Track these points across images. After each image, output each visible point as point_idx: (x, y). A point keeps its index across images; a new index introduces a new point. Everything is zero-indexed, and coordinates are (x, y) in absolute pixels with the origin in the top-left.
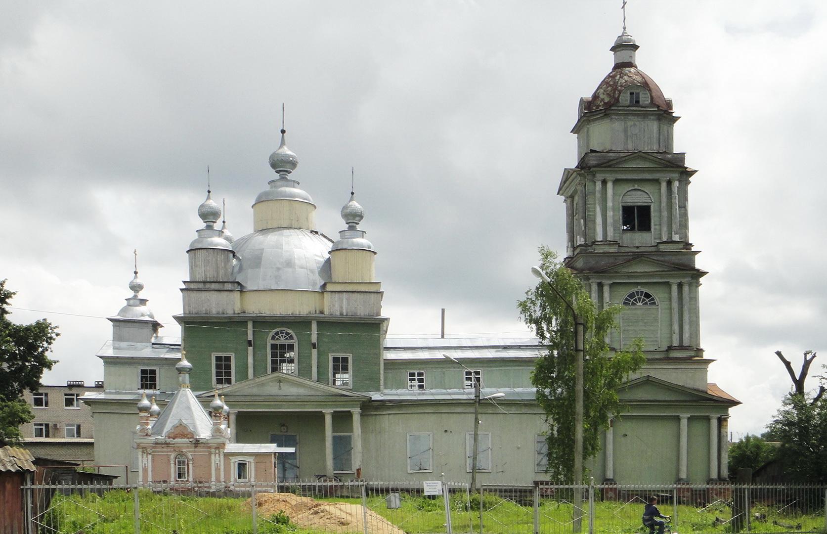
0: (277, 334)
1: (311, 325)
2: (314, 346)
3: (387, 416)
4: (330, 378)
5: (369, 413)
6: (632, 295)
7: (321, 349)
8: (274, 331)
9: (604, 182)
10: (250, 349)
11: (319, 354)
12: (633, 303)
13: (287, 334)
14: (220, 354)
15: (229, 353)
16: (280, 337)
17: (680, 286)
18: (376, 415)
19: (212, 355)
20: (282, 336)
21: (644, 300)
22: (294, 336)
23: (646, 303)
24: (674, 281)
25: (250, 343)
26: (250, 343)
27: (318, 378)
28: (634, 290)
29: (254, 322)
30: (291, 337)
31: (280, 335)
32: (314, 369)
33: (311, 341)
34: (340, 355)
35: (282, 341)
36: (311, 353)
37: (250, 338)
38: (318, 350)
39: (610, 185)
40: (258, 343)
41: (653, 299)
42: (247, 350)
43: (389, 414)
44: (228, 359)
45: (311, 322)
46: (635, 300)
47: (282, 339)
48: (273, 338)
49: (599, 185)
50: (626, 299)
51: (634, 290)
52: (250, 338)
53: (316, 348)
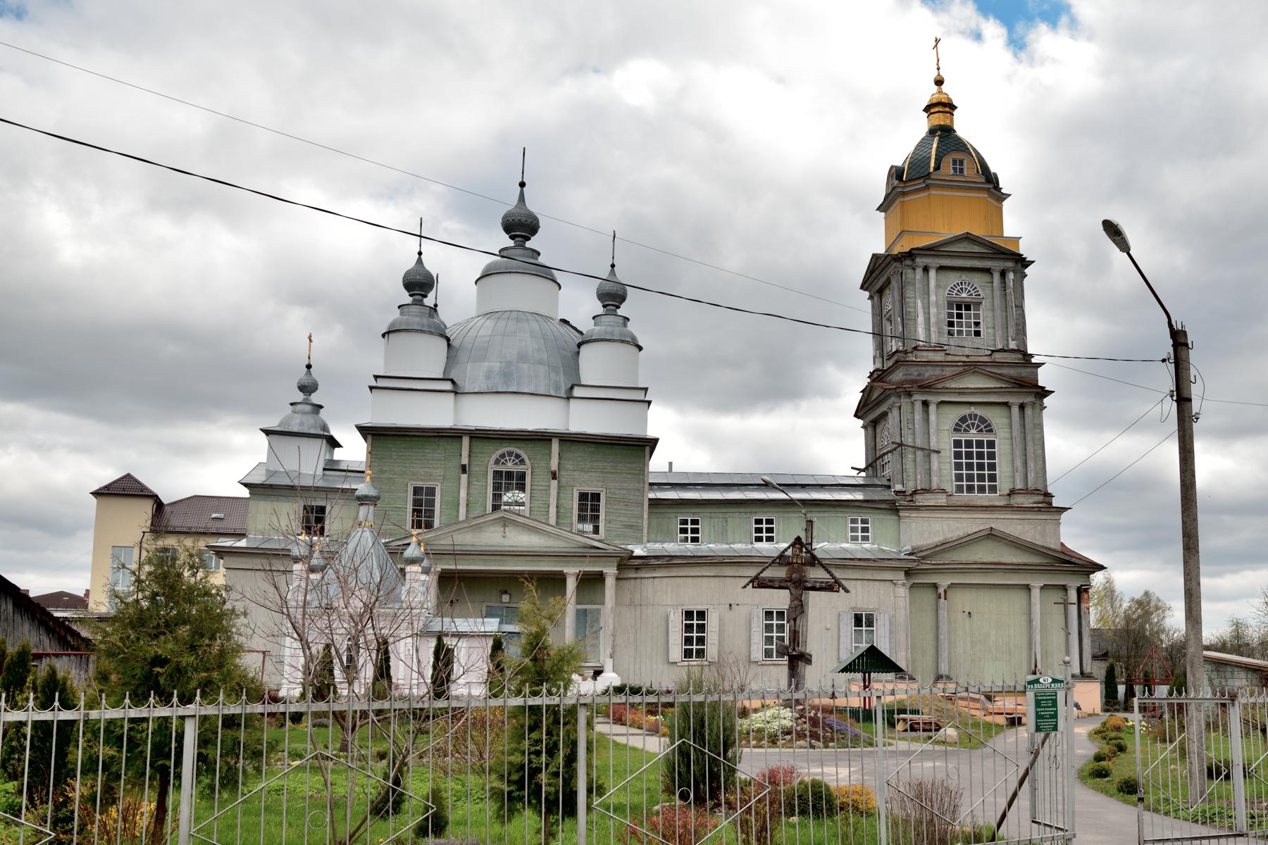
0: (503, 456)
2: (554, 476)
7: (563, 480)
10: (464, 477)
11: (559, 487)
13: (518, 456)
14: (420, 484)
15: (431, 483)
16: (506, 461)
18: (636, 578)
19: (409, 485)
20: (510, 460)
22: (527, 461)
25: (464, 469)
26: (464, 469)
27: (557, 523)
29: (471, 437)
30: (522, 462)
31: (507, 458)
32: (553, 510)
33: (549, 467)
34: (590, 489)
35: (510, 466)
36: (549, 486)
37: (465, 461)
38: (559, 482)
40: (474, 469)
42: (460, 478)
43: (654, 578)
44: (431, 491)
45: (551, 440)
47: (510, 464)
48: (497, 462)
52: (465, 461)
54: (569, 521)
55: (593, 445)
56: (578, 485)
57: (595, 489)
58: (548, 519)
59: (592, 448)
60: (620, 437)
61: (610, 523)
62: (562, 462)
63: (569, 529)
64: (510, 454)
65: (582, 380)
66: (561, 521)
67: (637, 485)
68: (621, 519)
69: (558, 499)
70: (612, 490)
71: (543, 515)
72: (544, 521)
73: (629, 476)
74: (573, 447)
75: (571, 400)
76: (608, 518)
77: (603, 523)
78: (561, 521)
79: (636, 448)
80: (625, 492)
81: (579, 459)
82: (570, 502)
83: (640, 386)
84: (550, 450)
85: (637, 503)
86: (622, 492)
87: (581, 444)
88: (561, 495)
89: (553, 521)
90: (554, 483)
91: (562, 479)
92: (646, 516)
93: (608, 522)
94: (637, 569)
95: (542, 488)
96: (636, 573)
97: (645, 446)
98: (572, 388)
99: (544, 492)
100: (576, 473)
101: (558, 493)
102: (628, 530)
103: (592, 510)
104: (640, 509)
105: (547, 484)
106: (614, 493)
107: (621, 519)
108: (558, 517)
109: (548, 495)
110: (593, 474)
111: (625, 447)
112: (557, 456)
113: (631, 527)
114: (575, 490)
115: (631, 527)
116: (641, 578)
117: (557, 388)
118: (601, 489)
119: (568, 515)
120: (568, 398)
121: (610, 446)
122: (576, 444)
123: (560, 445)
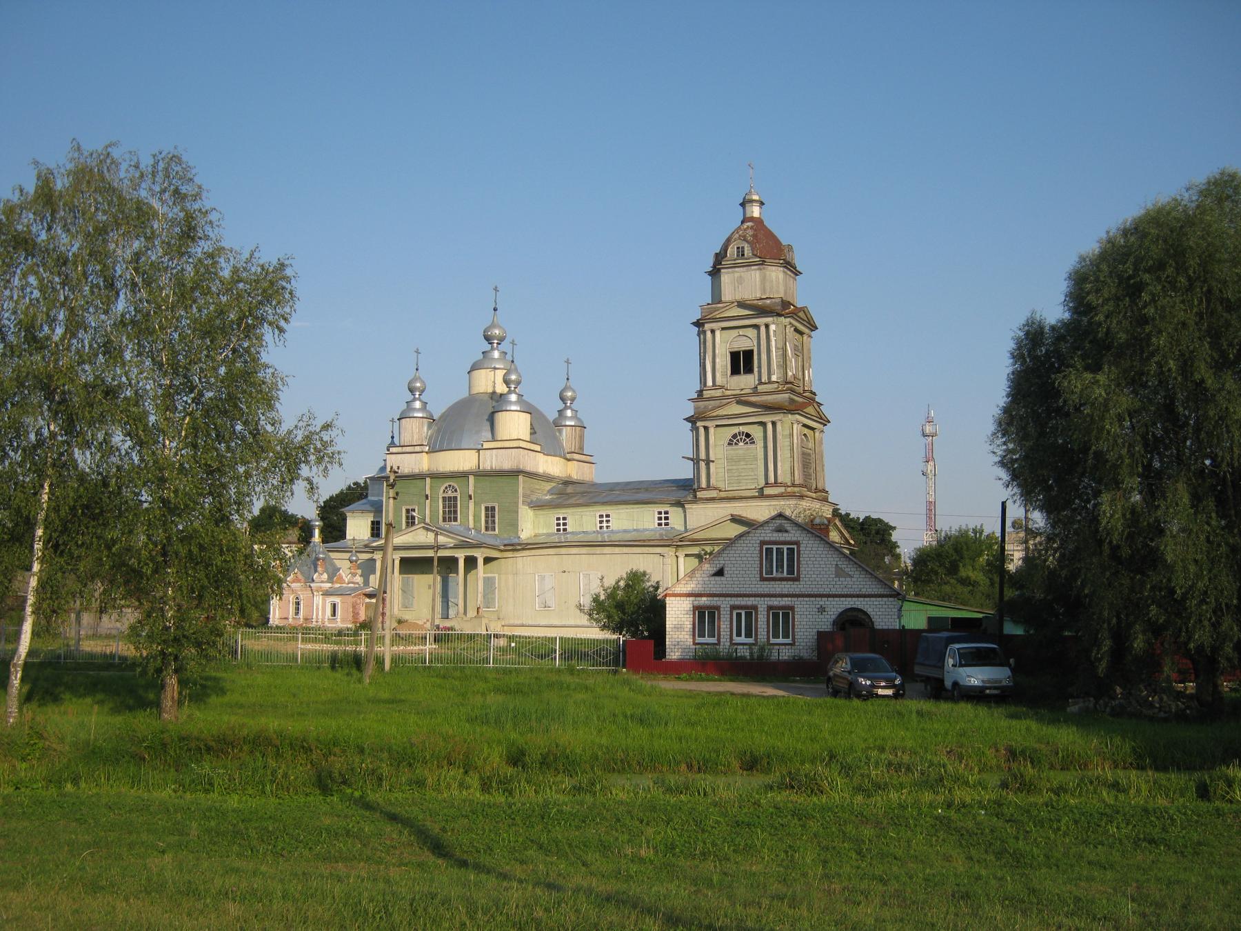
0: (446, 488)
6: (735, 436)
8: (447, 484)
9: (713, 331)
12: (736, 444)
17: (774, 424)
21: (745, 440)
23: (747, 443)
24: (767, 419)
28: (736, 430)
30: (456, 491)
35: (450, 494)
39: (718, 333)
41: (752, 439)
46: (738, 441)
47: (450, 492)
49: (709, 334)
50: (730, 440)
51: (736, 430)
64: (450, 486)
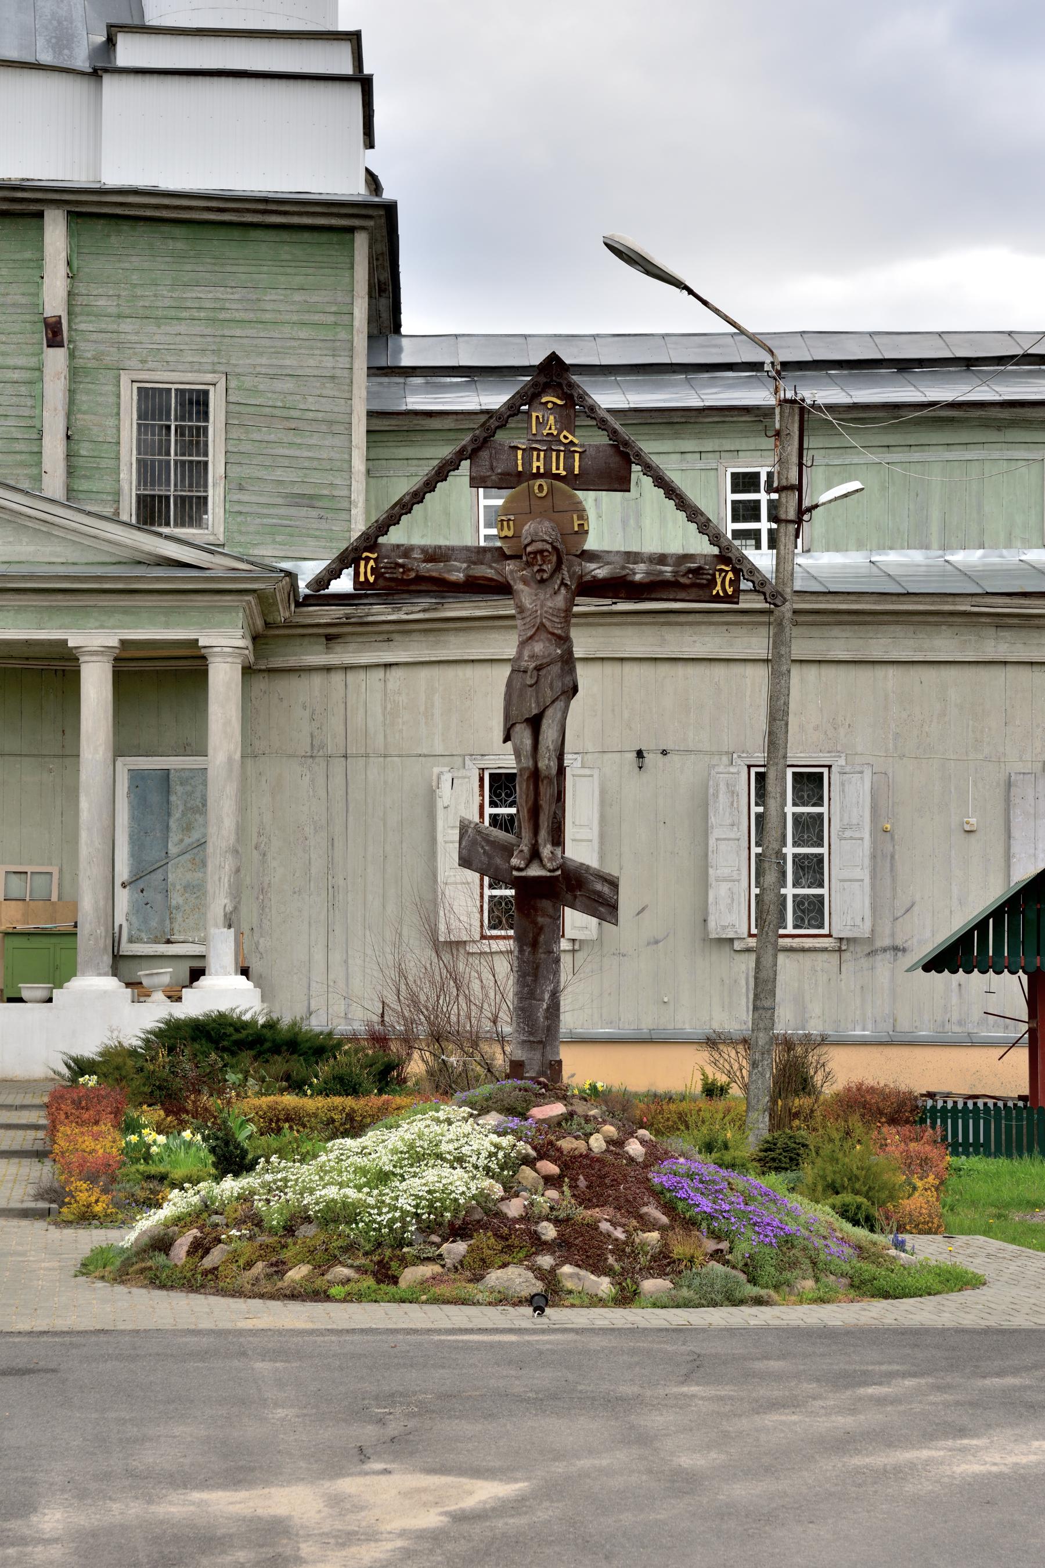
1: (41, 229)
2: (54, 334)
3: (380, 673)
4: (125, 486)
5: (292, 661)
7: (87, 350)
11: (75, 373)
18: (328, 669)
27: (70, 490)
32: (54, 449)
33: (37, 307)
36: (40, 369)
38: (72, 355)
43: (388, 666)
45: (40, 215)
53: (61, 345)
54: (107, 485)
55: (179, 231)
56: (134, 363)
57: (190, 377)
58: (38, 479)
59: (178, 242)
60: (266, 200)
61: (241, 488)
62: (81, 288)
63: (108, 511)
65: (146, 19)
66: (83, 485)
67: (329, 362)
68: (279, 474)
69: (69, 415)
70: (249, 382)
71: (23, 464)
72: (25, 485)
73: (302, 335)
74: (114, 240)
75: (107, 80)
76: (235, 471)
77: (220, 490)
78: (83, 485)
79: (324, 237)
80: (288, 385)
81: (135, 278)
82: (111, 422)
83: (342, 28)
84: (41, 249)
85: (331, 422)
86: (279, 385)
87: (142, 228)
88: (81, 397)
89: (54, 483)
90: (56, 359)
91: (82, 345)
92: (359, 464)
93: (235, 485)
94: (329, 638)
95: (16, 375)
96: (328, 649)
97: (351, 230)
98: (111, 42)
99: (23, 389)
100: (126, 326)
101: (72, 392)
102: (303, 511)
103: (185, 448)
104: (338, 441)
105: (33, 362)
106: (254, 391)
107: (279, 474)
108: (71, 471)
109: (39, 399)
110: (182, 328)
111: (285, 236)
112: (62, 269)
113: (308, 500)
114: (125, 379)
115: (308, 500)
116: (347, 668)
117: (62, 39)
118: (209, 377)
119: (104, 464)
120: (96, 74)
121: (236, 234)
122: (125, 227)
123: (71, 233)
